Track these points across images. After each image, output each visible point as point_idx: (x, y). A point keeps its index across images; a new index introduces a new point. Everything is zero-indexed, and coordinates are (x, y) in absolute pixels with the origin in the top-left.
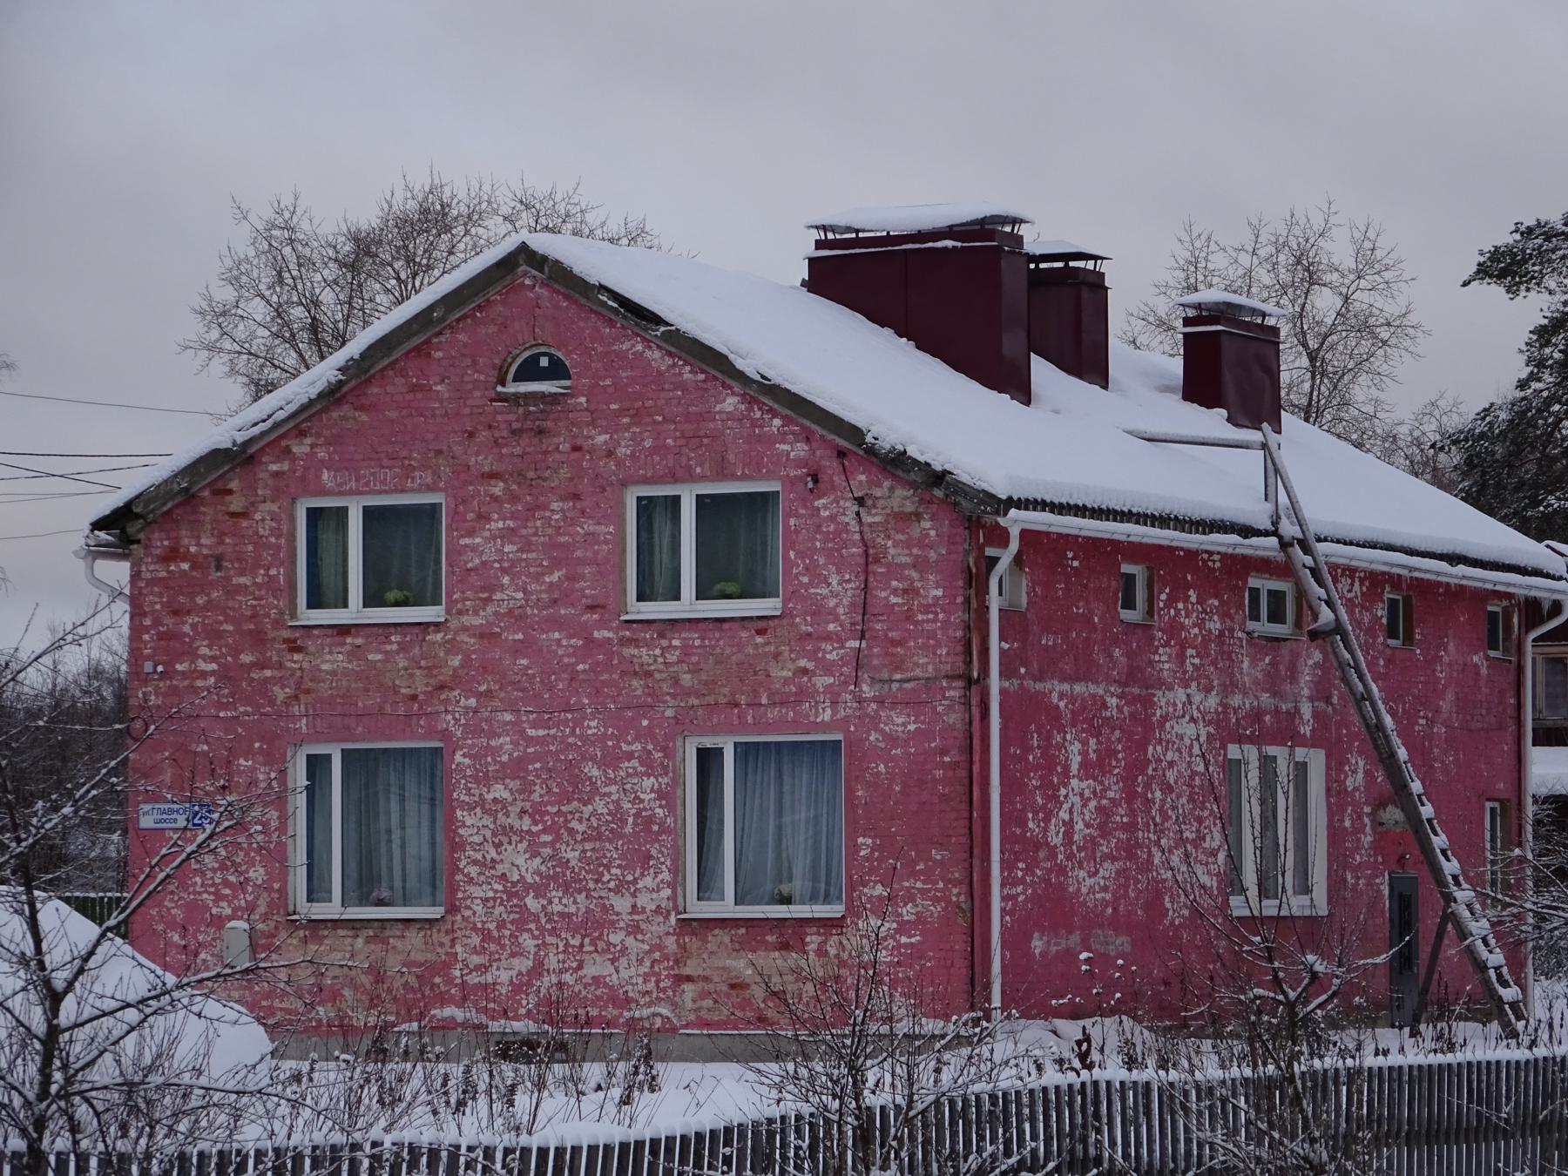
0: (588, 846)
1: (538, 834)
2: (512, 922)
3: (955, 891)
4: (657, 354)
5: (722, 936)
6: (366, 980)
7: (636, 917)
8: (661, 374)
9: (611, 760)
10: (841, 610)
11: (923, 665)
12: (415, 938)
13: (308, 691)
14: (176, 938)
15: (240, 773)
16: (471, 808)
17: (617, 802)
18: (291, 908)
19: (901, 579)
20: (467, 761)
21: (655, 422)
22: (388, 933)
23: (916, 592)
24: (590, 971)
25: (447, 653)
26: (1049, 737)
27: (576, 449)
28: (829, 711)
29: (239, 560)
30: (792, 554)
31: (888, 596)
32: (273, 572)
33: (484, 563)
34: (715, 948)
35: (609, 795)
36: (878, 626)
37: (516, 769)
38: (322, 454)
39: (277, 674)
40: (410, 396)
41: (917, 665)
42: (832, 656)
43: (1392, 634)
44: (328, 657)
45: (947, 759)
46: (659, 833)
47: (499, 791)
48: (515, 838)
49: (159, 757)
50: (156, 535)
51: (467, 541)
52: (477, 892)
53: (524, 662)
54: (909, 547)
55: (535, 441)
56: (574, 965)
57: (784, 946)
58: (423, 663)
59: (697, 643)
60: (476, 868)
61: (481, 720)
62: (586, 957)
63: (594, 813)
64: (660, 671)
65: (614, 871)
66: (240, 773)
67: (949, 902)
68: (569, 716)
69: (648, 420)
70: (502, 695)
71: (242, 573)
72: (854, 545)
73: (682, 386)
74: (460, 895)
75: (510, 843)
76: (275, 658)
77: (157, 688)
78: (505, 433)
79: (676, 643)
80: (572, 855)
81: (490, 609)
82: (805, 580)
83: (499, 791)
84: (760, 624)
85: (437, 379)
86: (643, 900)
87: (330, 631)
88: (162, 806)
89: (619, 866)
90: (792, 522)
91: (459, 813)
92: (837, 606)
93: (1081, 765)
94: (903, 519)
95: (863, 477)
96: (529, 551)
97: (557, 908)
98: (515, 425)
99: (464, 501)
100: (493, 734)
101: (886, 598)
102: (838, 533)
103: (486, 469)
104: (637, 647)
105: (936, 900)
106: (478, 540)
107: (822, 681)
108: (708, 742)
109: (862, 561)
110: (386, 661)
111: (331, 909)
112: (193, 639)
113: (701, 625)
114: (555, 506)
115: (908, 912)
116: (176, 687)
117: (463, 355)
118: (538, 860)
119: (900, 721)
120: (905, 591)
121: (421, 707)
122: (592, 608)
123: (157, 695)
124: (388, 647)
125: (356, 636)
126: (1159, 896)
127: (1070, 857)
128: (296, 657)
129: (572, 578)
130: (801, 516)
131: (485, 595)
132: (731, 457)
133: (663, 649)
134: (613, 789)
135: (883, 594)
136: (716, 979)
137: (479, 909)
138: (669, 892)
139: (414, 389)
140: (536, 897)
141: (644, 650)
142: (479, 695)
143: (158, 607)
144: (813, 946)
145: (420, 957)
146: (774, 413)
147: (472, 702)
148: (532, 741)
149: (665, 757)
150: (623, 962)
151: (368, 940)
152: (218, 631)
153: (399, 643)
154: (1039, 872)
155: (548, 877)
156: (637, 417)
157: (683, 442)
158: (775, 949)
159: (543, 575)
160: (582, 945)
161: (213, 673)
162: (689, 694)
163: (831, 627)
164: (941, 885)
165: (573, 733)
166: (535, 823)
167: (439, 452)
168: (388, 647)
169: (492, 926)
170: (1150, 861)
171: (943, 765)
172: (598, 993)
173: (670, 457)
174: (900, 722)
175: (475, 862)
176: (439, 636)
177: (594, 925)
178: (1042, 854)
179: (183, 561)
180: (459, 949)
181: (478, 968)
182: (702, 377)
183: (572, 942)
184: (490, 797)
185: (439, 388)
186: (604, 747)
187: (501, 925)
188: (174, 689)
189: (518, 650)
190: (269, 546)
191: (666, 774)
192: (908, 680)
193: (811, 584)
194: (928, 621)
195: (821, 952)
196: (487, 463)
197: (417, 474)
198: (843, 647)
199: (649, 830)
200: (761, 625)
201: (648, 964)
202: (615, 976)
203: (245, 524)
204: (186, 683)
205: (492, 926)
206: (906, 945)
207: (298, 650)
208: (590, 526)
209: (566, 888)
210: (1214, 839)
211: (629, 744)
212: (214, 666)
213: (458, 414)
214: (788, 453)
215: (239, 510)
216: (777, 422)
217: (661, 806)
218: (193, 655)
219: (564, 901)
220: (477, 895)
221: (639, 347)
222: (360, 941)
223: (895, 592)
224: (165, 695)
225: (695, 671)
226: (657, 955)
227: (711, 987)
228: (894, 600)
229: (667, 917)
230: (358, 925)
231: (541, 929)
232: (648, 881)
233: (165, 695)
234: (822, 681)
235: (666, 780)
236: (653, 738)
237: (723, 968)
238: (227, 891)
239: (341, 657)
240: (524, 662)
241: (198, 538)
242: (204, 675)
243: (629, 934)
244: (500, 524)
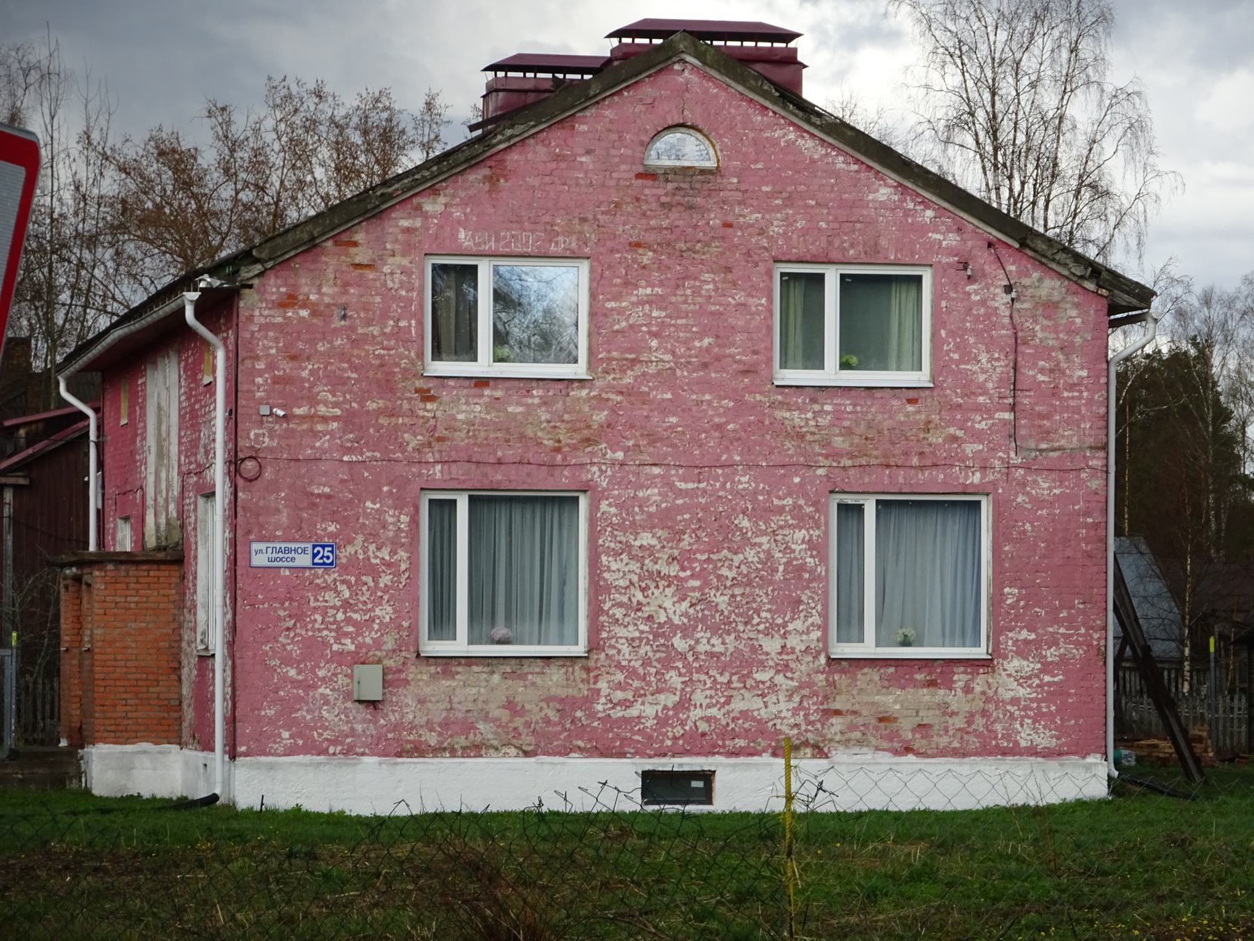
0: (738, 591)
1: (686, 579)
2: (658, 660)
3: (1096, 636)
4: (810, 143)
5: (874, 674)
6: (505, 715)
7: (785, 657)
8: (813, 161)
9: (763, 512)
10: (990, 385)
12: (556, 675)
13: (440, 439)
14: (292, 673)
15: (366, 515)
16: (616, 554)
17: (768, 552)
19: (1049, 358)
20: (613, 510)
21: (807, 206)
22: (526, 669)
23: (1063, 372)
24: (738, 705)
25: (593, 408)
28: (978, 475)
29: (365, 309)
30: (943, 333)
31: (1035, 374)
32: (403, 324)
33: (631, 326)
34: (864, 686)
35: (760, 545)
36: (1026, 401)
37: (664, 520)
38: (457, 214)
39: (406, 420)
40: (554, 165)
41: (1063, 436)
42: (983, 425)
44: (464, 408)
45: (1090, 520)
46: (810, 581)
47: (646, 539)
48: (662, 583)
49: (273, 497)
50: (272, 281)
51: (612, 304)
52: (621, 632)
53: (674, 420)
54: (1056, 332)
55: (685, 215)
56: (722, 700)
57: (932, 684)
58: (566, 417)
59: (849, 409)
60: (623, 611)
61: (628, 472)
62: (735, 693)
63: (745, 562)
64: (814, 434)
65: (764, 614)
66: (366, 515)
67: (1090, 645)
68: (720, 471)
69: (801, 203)
70: (651, 449)
71: (369, 323)
72: (1003, 327)
73: (837, 174)
74: (604, 635)
75: (657, 587)
76: (406, 406)
77: (271, 431)
78: (654, 206)
79: (828, 408)
80: (722, 600)
81: (639, 369)
82: (956, 356)
83: (646, 539)
84: (912, 395)
85: (581, 151)
86: (792, 641)
87: (467, 383)
88: (278, 545)
89: (769, 611)
90: (944, 304)
91: (604, 558)
92: (986, 381)
94: (1050, 307)
95: (1013, 268)
96: (678, 318)
97: (702, 647)
98: (663, 199)
99: (610, 267)
100: (641, 487)
101: (1034, 376)
102: (987, 316)
103: (634, 239)
104: (790, 410)
105: (1078, 644)
106: (624, 304)
107: (970, 448)
108: (850, 499)
110: (526, 414)
111: (459, 645)
112: (312, 386)
113: (853, 393)
114: (707, 277)
115: (1051, 654)
116: (293, 430)
117: (609, 130)
118: (685, 604)
119: (1047, 485)
120: (1051, 371)
121: (564, 459)
122: (745, 372)
123: (271, 438)
124: (530, 401)
125: (495, 388)
128: (429, 406)
130: (953, 299)
131: (633, 356)
132: (884, 242)
133: (814, 412)
134: (764, 539)
135: (1031, 373)
136: (864, 713)
137: (625, 649)
138: (819, 634)
139: (558, 158)
140: (684, 637)
141: (796, 413)
142: (627, 450)
143: (273, 351)
144: (961, 684)
145: (562, 693)
146: (926, 204)
147: (620, 455)
149: (817, 511)
150: (771, 699)
151: (505, 676)
152: (341, 378)
153: (541, 397)
155: (697, 620)
156: (789, 201)
157: (836, 225)
158: (924, 686)
159: (693, 339)
160: (730, 682)
161: (335, 418)
162: (842, 456)
163: (981, 399)
164: (1083, 631)
165: (723, 487)
166: (683, 569)
167: (584, 220)
168: (530, 401)
169: (637, 664)
171: (1086, 526)
172: (746, 725)
173: (824, 239)
174: (1044, 486)
175: (620, 605)
176: (584, 393)
177: (744, 664)
179: (304, 306)
180: (602, 685)
181: (620, 703)
182: (856, 167)
183: (720, 679)
184: (638, 543)
185: (584, 159)
186: (754, 501)
187: (646, 662)
188: (290, 434)
189: (664, 408)
190: (400, 298)
191: (818, 528)
192: (1053, 450)
193: (958, 363)
194: (1073, 398)
195: (968, 690)
197: (561, 238)
198: (991, 418)
199: (800, 577)
200: (912, 394)
201: (797, 699)
202: (763, 712)
203: (371, 275)
204: (305, 427)
205: (637, 664)
206: (1049, 684)
207: (432, 399)
208: (740, 297)
209: (715, 630)
211: (780, 498)
212: (338, 412)
213: (604, 185)
214: (940, 242)
215: (366, 262)
216: (929, 213)
217: (811, 556)
218: (313, 401)
219: (713, 641)
220: (624, 635)
221: (792, 136)
222: (496, 678)
223: (1042, 371)
224: (281, 437)
225: (849, 432)
226: (806, 692)
227: (860, 721)
228: (1041, 378)
229: (815, 657)
230: (495, 661)
231: (687, 666)
232: (798, 624)
233: (281, 437)
234: (970, 448)
235: (817, 533)
236: (805, 495)
237: (873, 703)
238: (351, 629)
239: (478, 408)
240: (674, 420)
241: (320, 287)
242: (325, 419)
243: (778, 672)
244: (649, 291)
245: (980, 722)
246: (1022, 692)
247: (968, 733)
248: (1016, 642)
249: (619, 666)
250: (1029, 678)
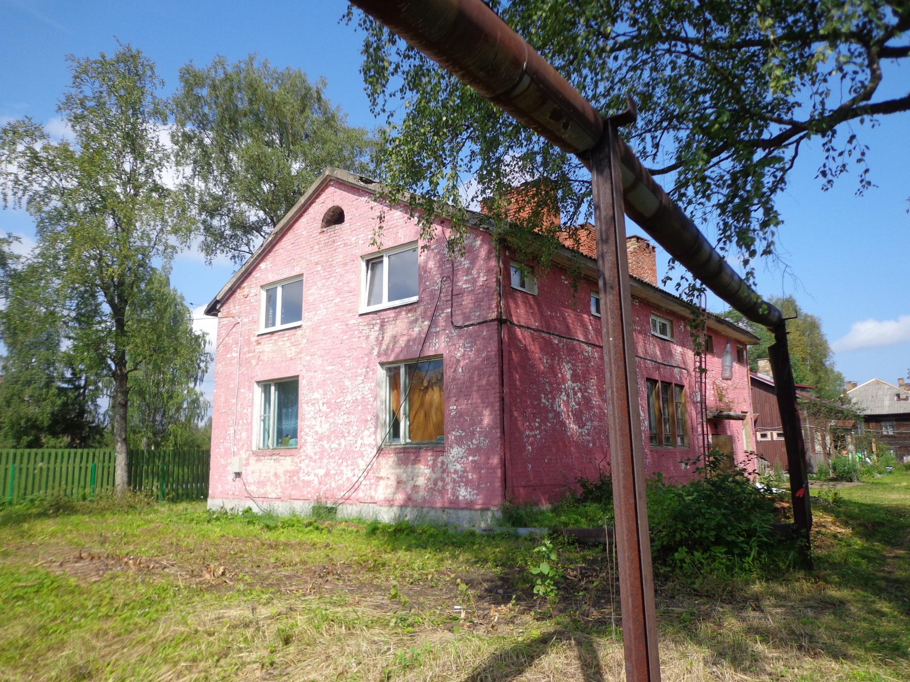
0: (346, 416)
47: (316, 395)
83: (316, 395)
93: (572, 376)
187: (315, 454)
196: (315, 258)
245: (440, 484)
246: (459, 467)
250: (462, 458)
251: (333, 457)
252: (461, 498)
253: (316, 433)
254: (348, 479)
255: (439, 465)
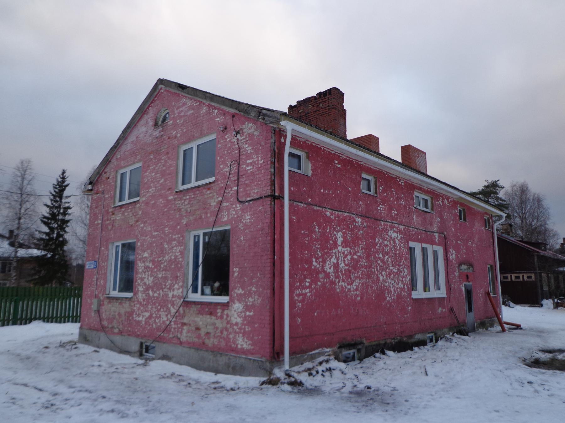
5: (194, 308)
11: (255, 192)
18: (107, 293)
26: (325, 229)
27: (169, 138)
43: (461, 219)
47: (146, 255)
57: (211, 314)
79: (188, 197)
83: (146, 255)
100: (146, 236)
109: (238, 155)
113: (194, 190)
126: (382, 292)
127: (338, 277)
129: (165, 181)
136: (192, 325)
146: (215, 108)
148: (154, 237)
154: (319, 283)
170: (378, 278)
178: (321, 276)
187: (144, 300)
206: (249, 316)
210: (406, 271)
245: (225, 333)
246: (239, 320)
247: (221, 338)
248: (237, 294)
249: (138, 301)
250: (241, 312)
251: (154, 304)
252: (239, 347)
253: (145, 284)
254: (164, 322)
255: (225, 317)
